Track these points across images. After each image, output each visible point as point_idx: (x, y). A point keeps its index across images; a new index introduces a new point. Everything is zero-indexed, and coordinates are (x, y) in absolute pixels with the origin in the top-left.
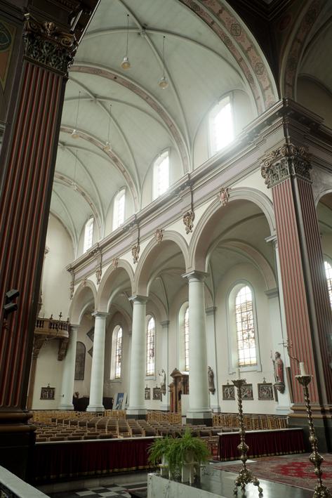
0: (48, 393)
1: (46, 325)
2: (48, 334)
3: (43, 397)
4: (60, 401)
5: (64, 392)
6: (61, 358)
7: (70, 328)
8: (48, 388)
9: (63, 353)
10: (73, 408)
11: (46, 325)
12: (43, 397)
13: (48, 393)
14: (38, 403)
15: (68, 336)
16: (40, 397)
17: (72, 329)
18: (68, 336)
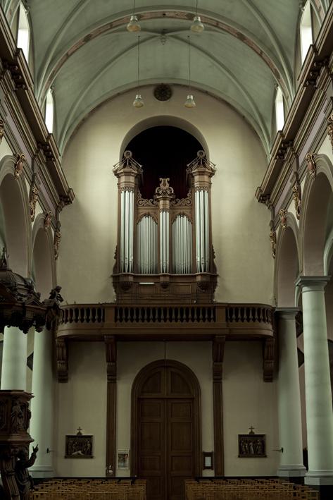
0: (253, 445)
1: (221, 315)
2: (227, 332)
3: (243, 453)
4: (278, 459)
5: (283, 444)
6: (271, 375)
7: (277, 317)
8: (252, 435)
9: (272, 365)
10: (305, 478)
11: (221, 315)
12: (243, 453)
13: (253, 445)
14: (235, 465)
15: (271, 333)
16: (237, 453)
17: (284, 316)
18: (271, 333)
